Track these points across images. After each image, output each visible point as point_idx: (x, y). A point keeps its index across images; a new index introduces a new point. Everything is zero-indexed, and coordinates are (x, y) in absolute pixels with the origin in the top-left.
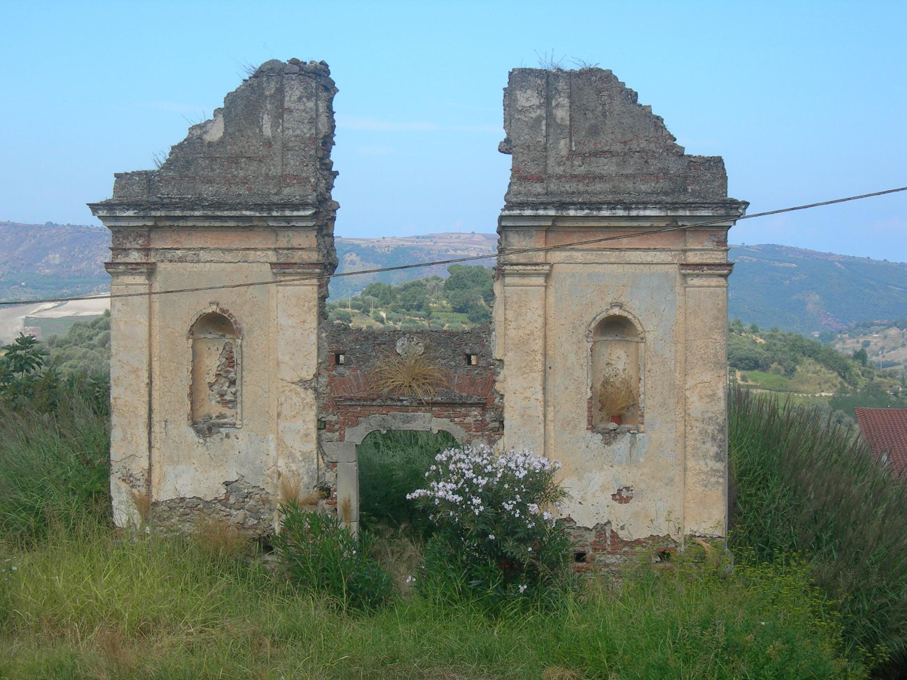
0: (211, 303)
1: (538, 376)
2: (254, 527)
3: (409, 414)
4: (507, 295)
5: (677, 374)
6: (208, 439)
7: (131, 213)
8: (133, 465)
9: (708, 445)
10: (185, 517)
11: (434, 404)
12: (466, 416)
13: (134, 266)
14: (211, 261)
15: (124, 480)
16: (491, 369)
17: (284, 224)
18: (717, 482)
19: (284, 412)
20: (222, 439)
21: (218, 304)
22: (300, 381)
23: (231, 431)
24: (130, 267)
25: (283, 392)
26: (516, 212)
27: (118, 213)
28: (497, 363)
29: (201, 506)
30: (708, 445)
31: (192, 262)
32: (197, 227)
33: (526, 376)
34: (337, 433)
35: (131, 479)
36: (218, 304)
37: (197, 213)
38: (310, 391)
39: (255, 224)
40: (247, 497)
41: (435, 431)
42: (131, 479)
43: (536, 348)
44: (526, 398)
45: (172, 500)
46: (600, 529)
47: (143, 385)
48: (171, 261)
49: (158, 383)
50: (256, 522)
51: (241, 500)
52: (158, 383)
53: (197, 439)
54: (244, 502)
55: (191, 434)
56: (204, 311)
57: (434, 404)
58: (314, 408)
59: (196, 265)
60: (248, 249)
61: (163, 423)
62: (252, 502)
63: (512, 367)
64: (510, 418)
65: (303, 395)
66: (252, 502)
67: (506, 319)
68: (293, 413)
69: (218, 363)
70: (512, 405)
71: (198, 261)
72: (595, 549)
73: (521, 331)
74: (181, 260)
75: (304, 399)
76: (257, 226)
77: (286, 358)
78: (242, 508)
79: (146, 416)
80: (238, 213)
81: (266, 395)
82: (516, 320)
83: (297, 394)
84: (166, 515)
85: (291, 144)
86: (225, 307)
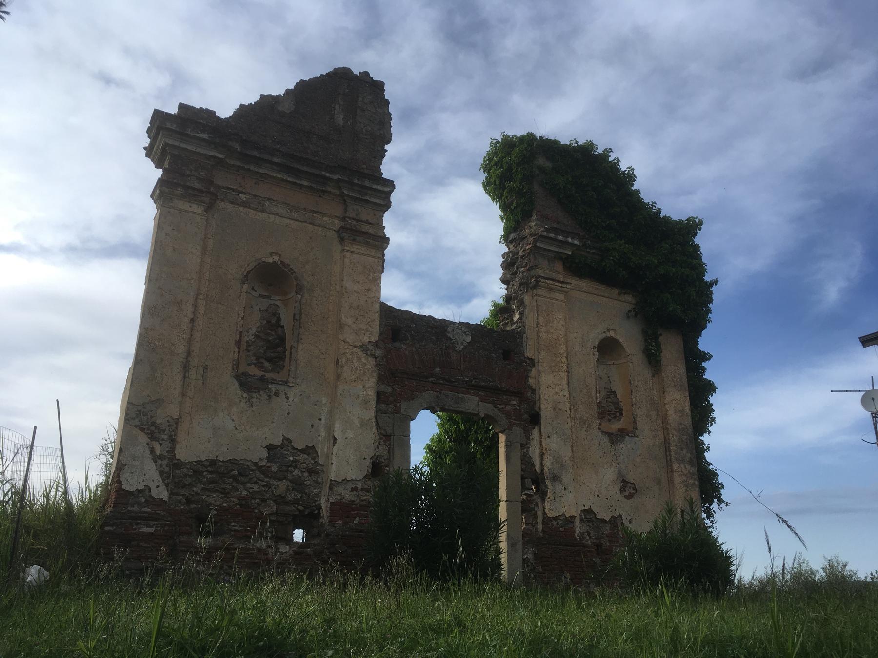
0: (272, 254)
1: (564, 375)
2: (296, 502)
3: (460, 395)
6: (254, 395)
7: (205, 136)
9: (684, 452)
14: (277, 214)
15: (142, 430)
17: (358, 196)
18: (694, 484)
20: (269, 396)
22: (361, 347)
23: (282, 388)
24: (190, 191)
25: (344, 354)
26: (552, 235)
28: (528, 361)
31: (255, 209)
34: (392, 406)
35: (153, 428)
37: (275, 160)
39: (329, 189)
40: (291, 466)
42: (153, 428)
43: (562, 352)
45: (199, 462)
46: (615, 521)
47: (186, 320)
48: (232, 203)
49: (200, 323)
50: (299, 496)
51: (285, 468)
52: (200, 323)
53: (240, 392)
54: (287, 471)
56: (264, 259)
59: (260, 214)
60: (316, 212)
61: (201, 369)
62: (296, 472)
64: (546, 411)
65: (363, 360)
66: (296, 472)
68: (353, 377)
69: (259, 324)
71: (263, 211)
74: (245, 204)
76: (330, 192)
77: (350, 321)
78: (285, 478)
80: (317, 172)
83: (359, 358)
84: (188, 480)
86: (287, 261)
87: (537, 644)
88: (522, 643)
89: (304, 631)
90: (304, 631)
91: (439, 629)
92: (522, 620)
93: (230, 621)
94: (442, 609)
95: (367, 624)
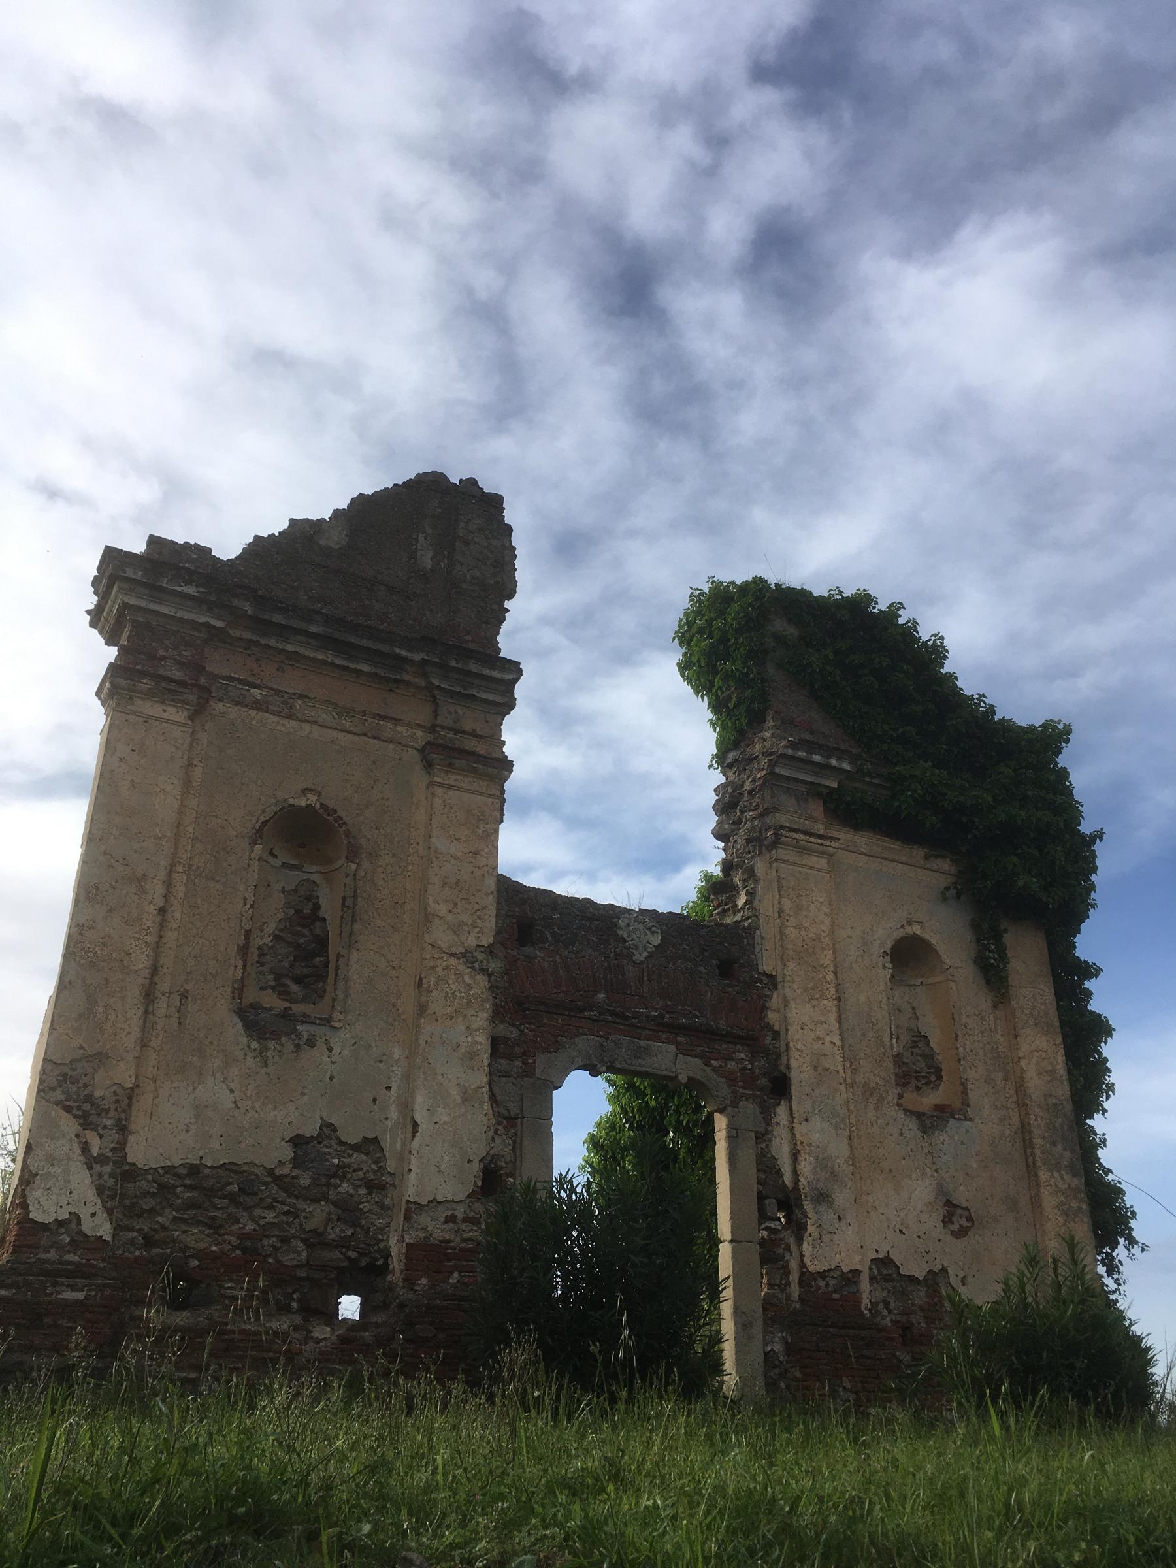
0: (305, 791)
1: (831, 1004)
2: (343, 1244)
3: (643, 1043)
6: (271, 1044)
7: (191, 590)
9: (1060, 1147)
12: (728, 1058)
13: (174, 686)
14: (315, 722)
15: (68, 1109)
17: (458, 689)
18: (1080, 1208)
19: (433, 1007)
20: (298, 1046)
21: (320, 794)
22: (463, 955)
24: (164, 684)
25: (433, 968)
28: (765, 980)
30: (1060, 1147)
31: (278, 714)
33: (814, 1002)
34: (518, 1063)
35: (87, 1107)
36: (320, 794)
37: (313, 629)
39: (407, 678)
40: (335, 1175)
41: (683, 1078)
42: (87, 1107)
43: (826, 962)
44: (818, 1038)
46: (935, 1279)
47: (152, 909)
48: (237, 703)
49: (178, 915)
51: (324, 1180)
52: (178, 915)
54: (328, 1185)
58: (487, 1006)
59: (285, 721)
60: (384, 718)
62: (345, 1187)
63: (795, 986)
64: (800, 1070)
65: (467, 979)
67: (780, 912)
69: (281, 915)
70: (799, 1046)
71: (290, 717)
74: (258, 706)
76: (408, 683)
77: (442, 909)
79: (146, 973)
81: (394, 973)
83: (460, 976)
84: (147, 1203)
86: (331, 804)
87: (747, 1513)
88: (721, 1513)
89: (328, 1487)
90: (328, 1487)
91: (575, 1488)
92: (734, 1468)
93: (183, 1466)
94: (585, 1447)
95: (445, 1474)
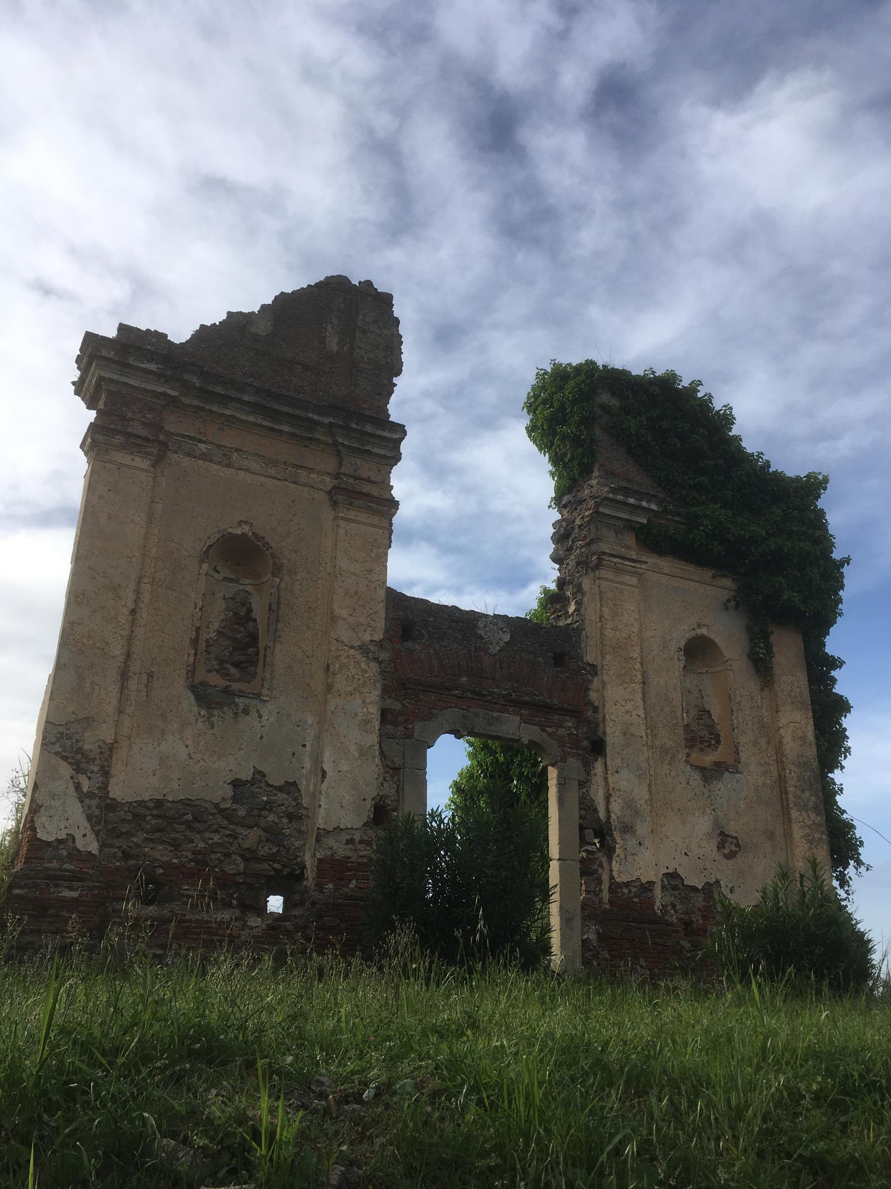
0: (240, 523)
1: (638, 687)
2: (271, 858)
3: (495, 714)
4: (603, 590)
5: (764, 711)
6: (215, 712)
7: (153, 367)
8: (87, 734)
9: (807, 794)
10: (157, 835)
11: (524, 704)
12: (559, 726)
13: (140, 442)
14: (248, 470)
15: (65, 759)
16: (582, 675)
19: (337, 686)
20: (236, 714)
21: (251, 525)
22: (360, 647)
23: (253, 703)
25: (338, 657)
26: (620, 497)
27: (131, 361)
28: (588, 668)
29: (189, 817)
30: (807, 794)
31: (219, 464)
32: (239, 419)
33: (625, 685)
34: (401, 728)
35: (79, 756)
36: (251, 525)
37: (246, 398)
38: (64, 836)
39: (317, 436)
40: (264, 809)
41: (525, 741)
42: (79, 756)
43: (635, 655)
44: (628, 712)
45: (141, 803)
46: (710, 889)
47: (125, 611)
48: (188, 455)
50: (275, 850)
51: (256, 812)
53: (196, 709)
54: (259, 816)
55: (188, 701)
56: (230, 530)
57: (524, 704)
58: (378, 685)
59: (225, 469)
61: (145, 677)
62: (272, 817)
63: (611, 673)
64: (613, 736)
65: (363, 666)
66: (272, 817)
67: (601, 617)
68: (349, 689)
69: (222, 617)
70: (613, 717)
71: (229, 465)
72: (705, 918)
73: (618, 633)
74: (205, 457)
75: (365, 671)
77: (345, 613)
78: (257, 825)
79: (122, 658)
80: (302, 414)
81: (307, 661)
82: (612, 620)
83: (358, 663)
84: (125, 828)
85: (362, 365)
86: (260, 533)
87: (570, 1052)
88: (551, 1051)
89: (261, 1030)
90: (261, 1030)
91: (442, 1033)
92: (560, 1020)
93: (154, 1013)
94: (451, 1004)
95: (347, 1022)
